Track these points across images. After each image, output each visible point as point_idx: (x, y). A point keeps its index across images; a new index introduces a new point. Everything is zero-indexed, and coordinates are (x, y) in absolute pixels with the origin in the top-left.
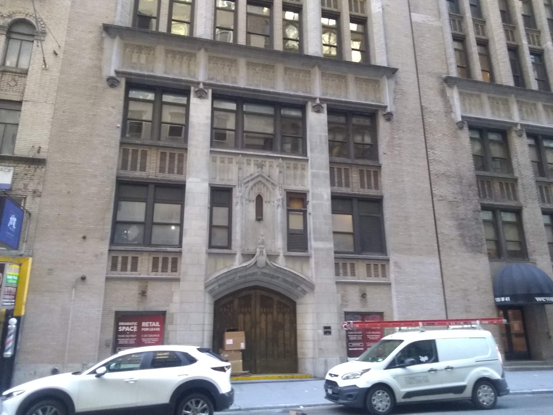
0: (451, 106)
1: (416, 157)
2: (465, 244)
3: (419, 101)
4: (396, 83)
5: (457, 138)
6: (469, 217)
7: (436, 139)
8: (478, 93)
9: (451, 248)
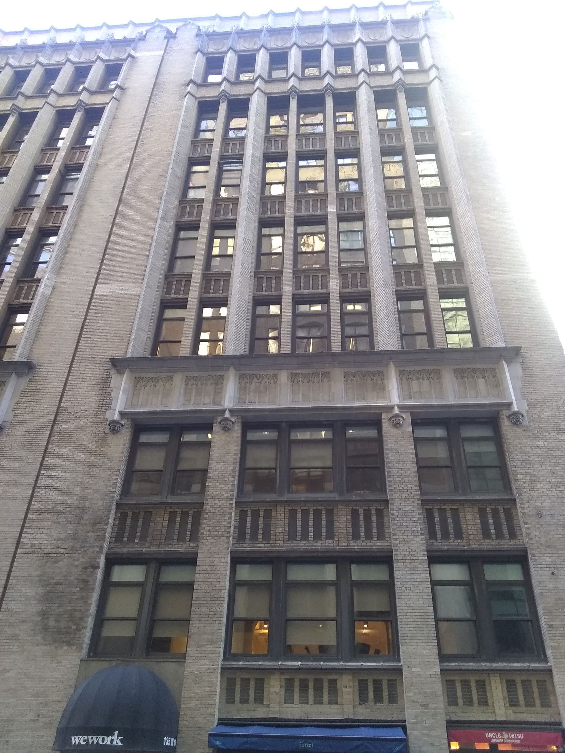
0: (111, 400)
1: (14, 486)
2: (45, 628)
3: (58, 401)
4: (31, 380)
5: (102, 447)
6: (72, 578)
7: (62, 454)
8: (168, 374)
9: (14, 637)
